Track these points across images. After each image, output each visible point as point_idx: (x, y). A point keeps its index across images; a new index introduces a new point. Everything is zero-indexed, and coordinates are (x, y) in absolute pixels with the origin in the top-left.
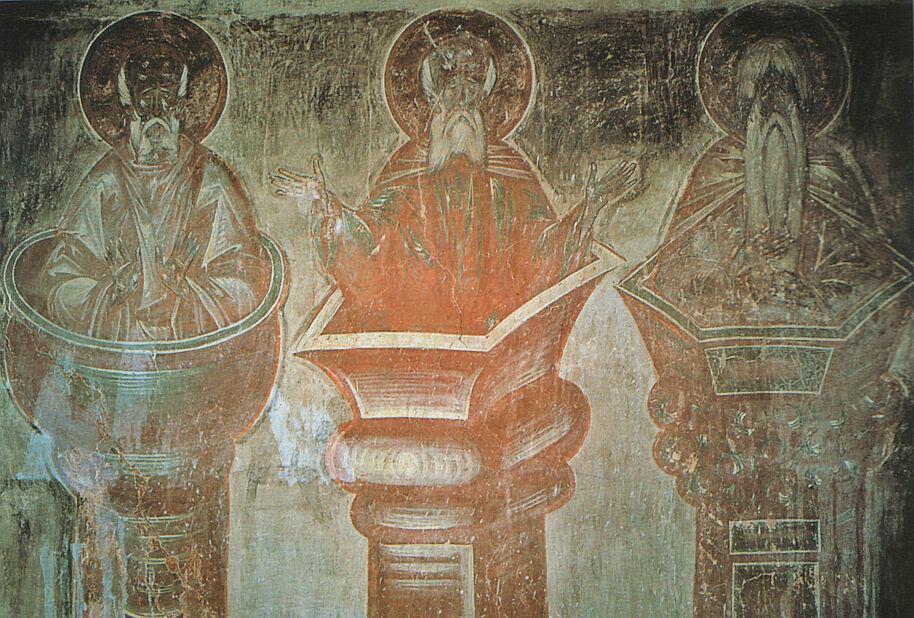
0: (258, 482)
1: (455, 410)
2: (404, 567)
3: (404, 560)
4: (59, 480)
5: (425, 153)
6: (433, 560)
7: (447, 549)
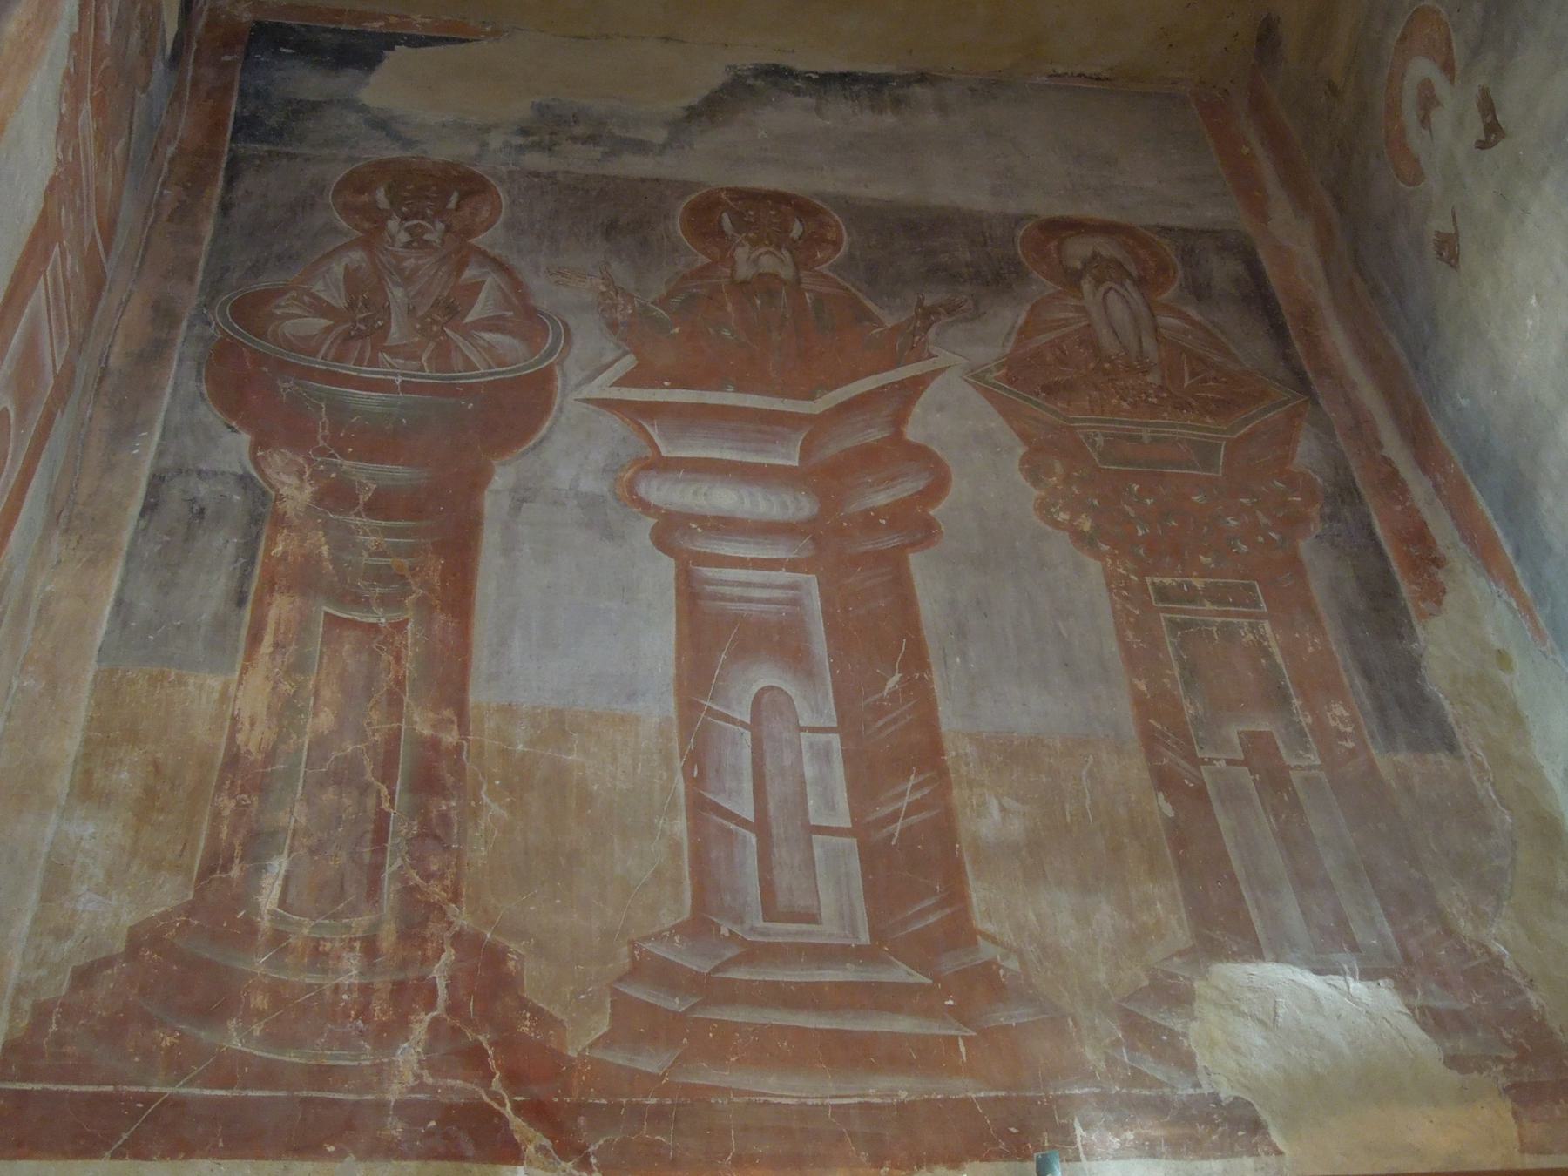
0: (524, 500)
1: (787, 456)
2: (727, 590)
3: (724, 583)
4: (255, 474)
5: (728, 271)
6: (763, 586)
7: (783, 576)
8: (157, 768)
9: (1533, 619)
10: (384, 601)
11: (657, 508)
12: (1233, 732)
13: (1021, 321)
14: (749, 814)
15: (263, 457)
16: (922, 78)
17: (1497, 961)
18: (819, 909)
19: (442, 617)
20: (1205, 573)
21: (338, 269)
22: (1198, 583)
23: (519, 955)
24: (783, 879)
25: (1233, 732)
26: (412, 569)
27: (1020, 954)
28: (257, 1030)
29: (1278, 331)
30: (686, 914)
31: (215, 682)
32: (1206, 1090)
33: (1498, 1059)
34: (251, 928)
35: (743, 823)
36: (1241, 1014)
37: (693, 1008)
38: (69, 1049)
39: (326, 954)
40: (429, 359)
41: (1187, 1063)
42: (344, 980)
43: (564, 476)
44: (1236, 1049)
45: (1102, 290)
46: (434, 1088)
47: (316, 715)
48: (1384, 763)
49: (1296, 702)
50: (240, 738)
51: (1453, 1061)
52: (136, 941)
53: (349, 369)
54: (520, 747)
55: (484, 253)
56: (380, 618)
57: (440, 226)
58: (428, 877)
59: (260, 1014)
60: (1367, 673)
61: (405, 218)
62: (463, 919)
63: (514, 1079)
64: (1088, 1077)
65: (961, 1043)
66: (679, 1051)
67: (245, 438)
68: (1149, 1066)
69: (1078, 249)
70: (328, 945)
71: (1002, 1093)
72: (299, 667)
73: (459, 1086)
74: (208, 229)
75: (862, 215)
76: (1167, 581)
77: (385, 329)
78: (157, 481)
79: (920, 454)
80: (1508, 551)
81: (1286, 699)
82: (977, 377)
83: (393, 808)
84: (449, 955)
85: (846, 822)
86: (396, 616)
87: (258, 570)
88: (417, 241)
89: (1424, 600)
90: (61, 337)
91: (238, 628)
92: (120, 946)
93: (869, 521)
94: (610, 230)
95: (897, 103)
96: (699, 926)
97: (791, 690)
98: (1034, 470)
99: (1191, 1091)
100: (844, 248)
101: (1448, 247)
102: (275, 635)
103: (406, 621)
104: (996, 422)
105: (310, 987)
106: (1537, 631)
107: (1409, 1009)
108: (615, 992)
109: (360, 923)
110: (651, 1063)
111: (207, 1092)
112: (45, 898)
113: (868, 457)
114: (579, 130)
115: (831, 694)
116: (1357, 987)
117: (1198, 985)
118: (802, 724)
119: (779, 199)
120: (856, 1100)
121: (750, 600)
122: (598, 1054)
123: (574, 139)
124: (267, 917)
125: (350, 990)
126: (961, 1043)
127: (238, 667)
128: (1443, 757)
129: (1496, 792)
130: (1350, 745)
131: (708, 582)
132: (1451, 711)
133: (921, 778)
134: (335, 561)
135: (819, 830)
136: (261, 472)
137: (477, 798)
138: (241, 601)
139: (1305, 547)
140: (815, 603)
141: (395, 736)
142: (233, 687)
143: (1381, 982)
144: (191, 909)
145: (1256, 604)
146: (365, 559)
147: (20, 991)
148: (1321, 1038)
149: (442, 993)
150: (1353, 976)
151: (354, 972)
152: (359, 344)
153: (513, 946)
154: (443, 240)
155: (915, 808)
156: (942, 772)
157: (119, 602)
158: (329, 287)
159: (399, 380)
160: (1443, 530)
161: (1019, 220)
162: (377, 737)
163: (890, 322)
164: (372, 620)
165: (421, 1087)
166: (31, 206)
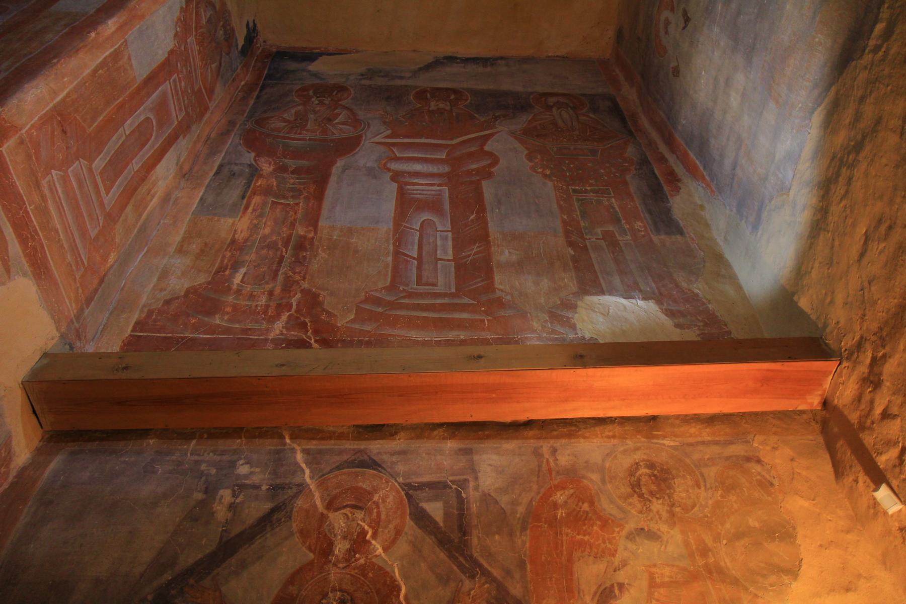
2: (415, 192)
6: (428, 190)
8: (206, 244)
9: (711, 189)
10: (293, 197)
11: (393, 170)
12: (599, 230)
13: (530, 118)
14: (415, 255)
15: (258, 159)
16: (502, 58)
17: (697, 295)
18: (437, 282)
19: (313, 201)
20: (591, 185)
21: (293, 111)
22: (588, 188)
23: (324, 295)
24: (425, 274)
25: (599, 230)
26: (304, 188)
27: (512, 295)
28: (226, 318)
29: (622, 119)
30: (388, 284)
31: (230, 221)
32: (580, 335)
33: (696, 326)
34: (229, 288)
35: (413, 258)
36: (594, 311)
37: (385, 311)
38: (158, 323)
39: (255, 296)
40: (319, 133)
41: (573, 327)
42: (260, 303)
43: (362, 162)
44: (592, 322)
45: (559, 110)
46: (286, 334)
47: (264, 229)
48: (655, 239)
49: (623, 222)
50: (236, 236)
51: (677, 326)
52: (188, 292)
53: (292, 136)
54: (335, 237)
55: (344, 106)
56: (291, 202)
57: (329, 99)
58: (295, 273)
59: (228, 313)
60: (650, 212)
61: (318, 97)
62: (305, 285)
63: (316, 332)
64: (534, 331)
65: (486, 321)
66: (379, 324)
67: (253, 154)
68: (558, 328)
69: (551, 100)
70: (256, 293)
71: (501, 336)
72: (261, 216)
73: (296, 334)
74: (251, 102)
75: (474, 92)
76: (577, 187)
77: (306, 125)
78: (221, 167)
79: (490, 154)
80: (701, 168)
81: (619, 221)
82: (512, 134)
83: (286, 254)
84: (299, 295)
85: (451, 257)
86: (297, 201)
87: (250, 190)
88: (321, 103)
89: (672, 191)
90: (180, 109)
91: (241, 205)
92: (182, 293)
93: (469, 173)
94: (388, 99)
95: (492, 65)
96: (392, 288)
97: (435, 220)
98: (530, 157)
99: (574, 336)
100: (469, 101)
101: (676, 72)
102: (254, 206)
103: (300, 203)
104: (517, 145)
105: (247, 305)
106: (712, 192)
107: (660, 309)
108: (357, 306)
109: (268, 287)
110: (367, 328)
111: (205, 336)
112: (159, 280)
113: (471, 155)
114: (382, 74)
115: (449, 221)
116: (641, 303)
117: (579, 303)
118: (438, 229)
119: (447, 89)
120: (444, 339)
121: (423, 195)
122: (348, 325)
123: (379, 76)
124: (235, 285)
125: (261, 306)
126: (486, 321)
127: (239, 216)
128: (679, 237)
129: (698, 246)
130: (643, 233)
131: (409, 190)
132: (682, 224)
133: (480, 244)
134: (278, 186)
135: (440, 260)
136: (256, 163)
137: (317, 252)
138: (243, 197)
139: (628, 177)
140: (447, 195)
141: (291, 235)
142: (236, 223)
143: (650, 301)
144: (209, 283)
145: (610, 194)
146: (288, 186)
147: (144, 306)
148: (626, 319)
149: (294, 307)
150: (639, 299)
151: (264, 301)
152: (296, 129)
153: (322, 293)
154: (330, 103)
155: (476, 253)
156: (488, 243)
157: (202, 199)
158: (289, 115)
159: (308, 138)
160: (679, 170)
161: (532, 93)
162: (285, 235)
163: (483, 119)
164: (288, 202)
165: (282, 334)
166: (161, 56)
